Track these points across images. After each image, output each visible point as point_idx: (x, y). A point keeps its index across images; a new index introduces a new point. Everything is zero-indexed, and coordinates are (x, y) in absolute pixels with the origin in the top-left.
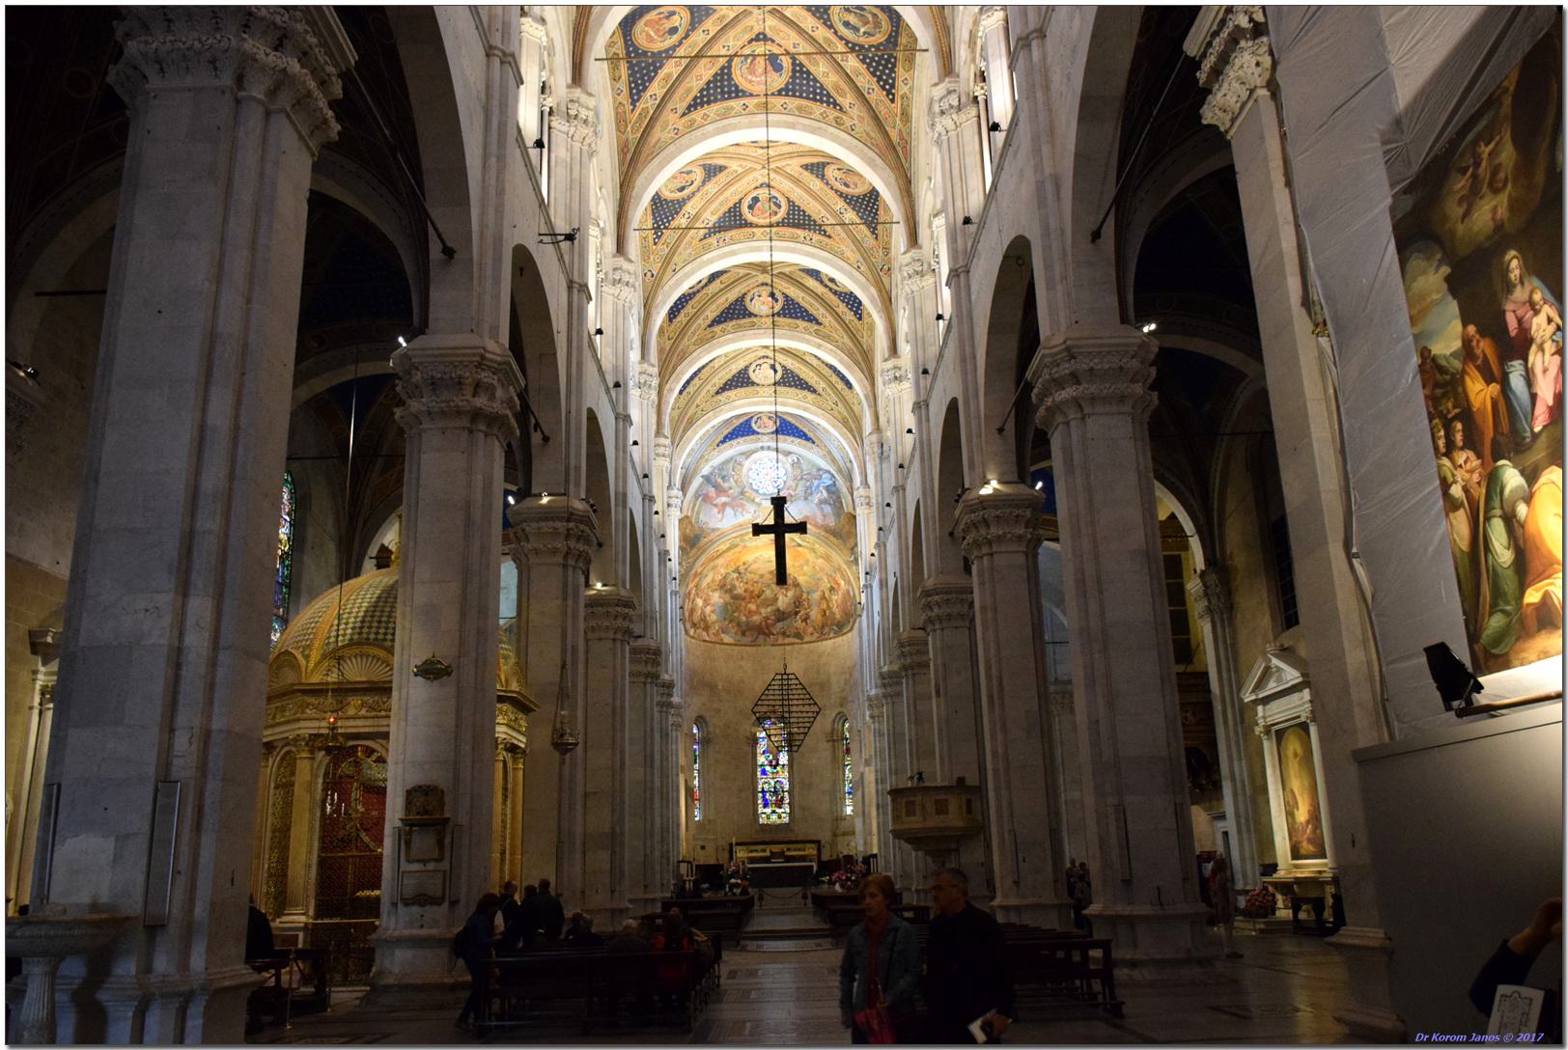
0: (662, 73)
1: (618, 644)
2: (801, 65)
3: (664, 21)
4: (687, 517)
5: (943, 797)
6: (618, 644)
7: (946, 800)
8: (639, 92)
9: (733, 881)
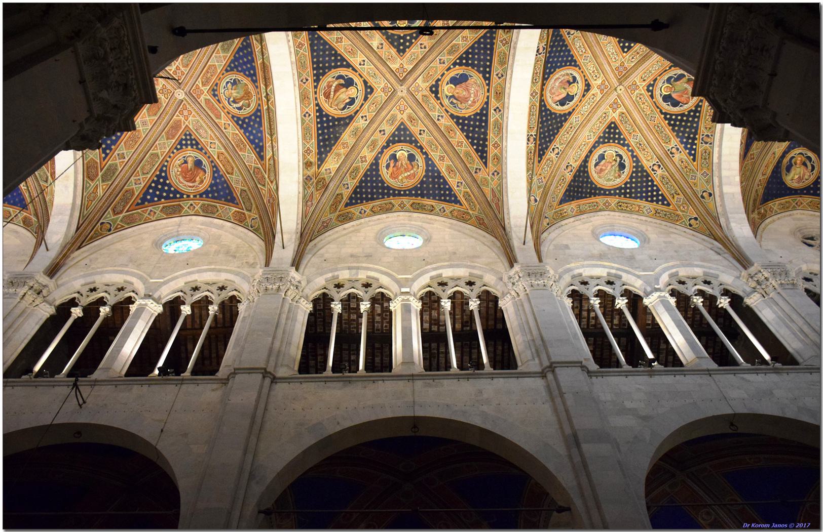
0: (444, 172)
2: (461, 58)
3: (399, 164)
8: (450, 195)
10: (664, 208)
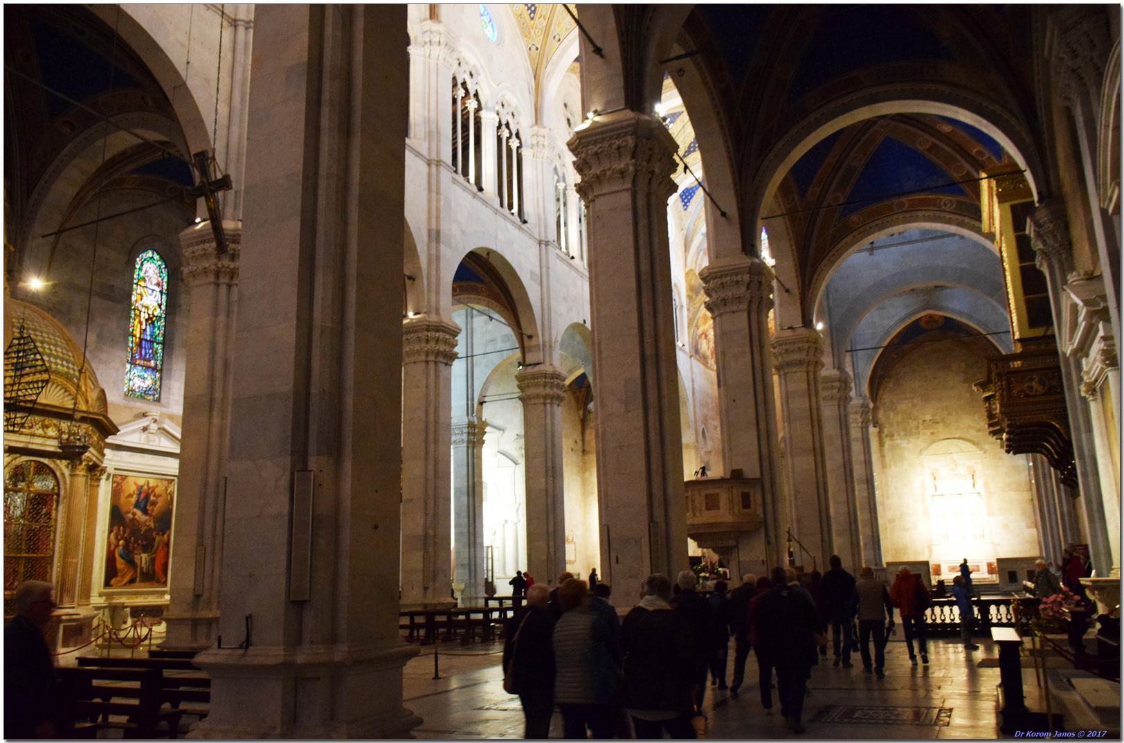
1: (432, 366)
4: (691, 270)
5: (716, 491)
6: (432, 366)
7: (717, 495)
9: (702, 574)
10: (528, 18)
